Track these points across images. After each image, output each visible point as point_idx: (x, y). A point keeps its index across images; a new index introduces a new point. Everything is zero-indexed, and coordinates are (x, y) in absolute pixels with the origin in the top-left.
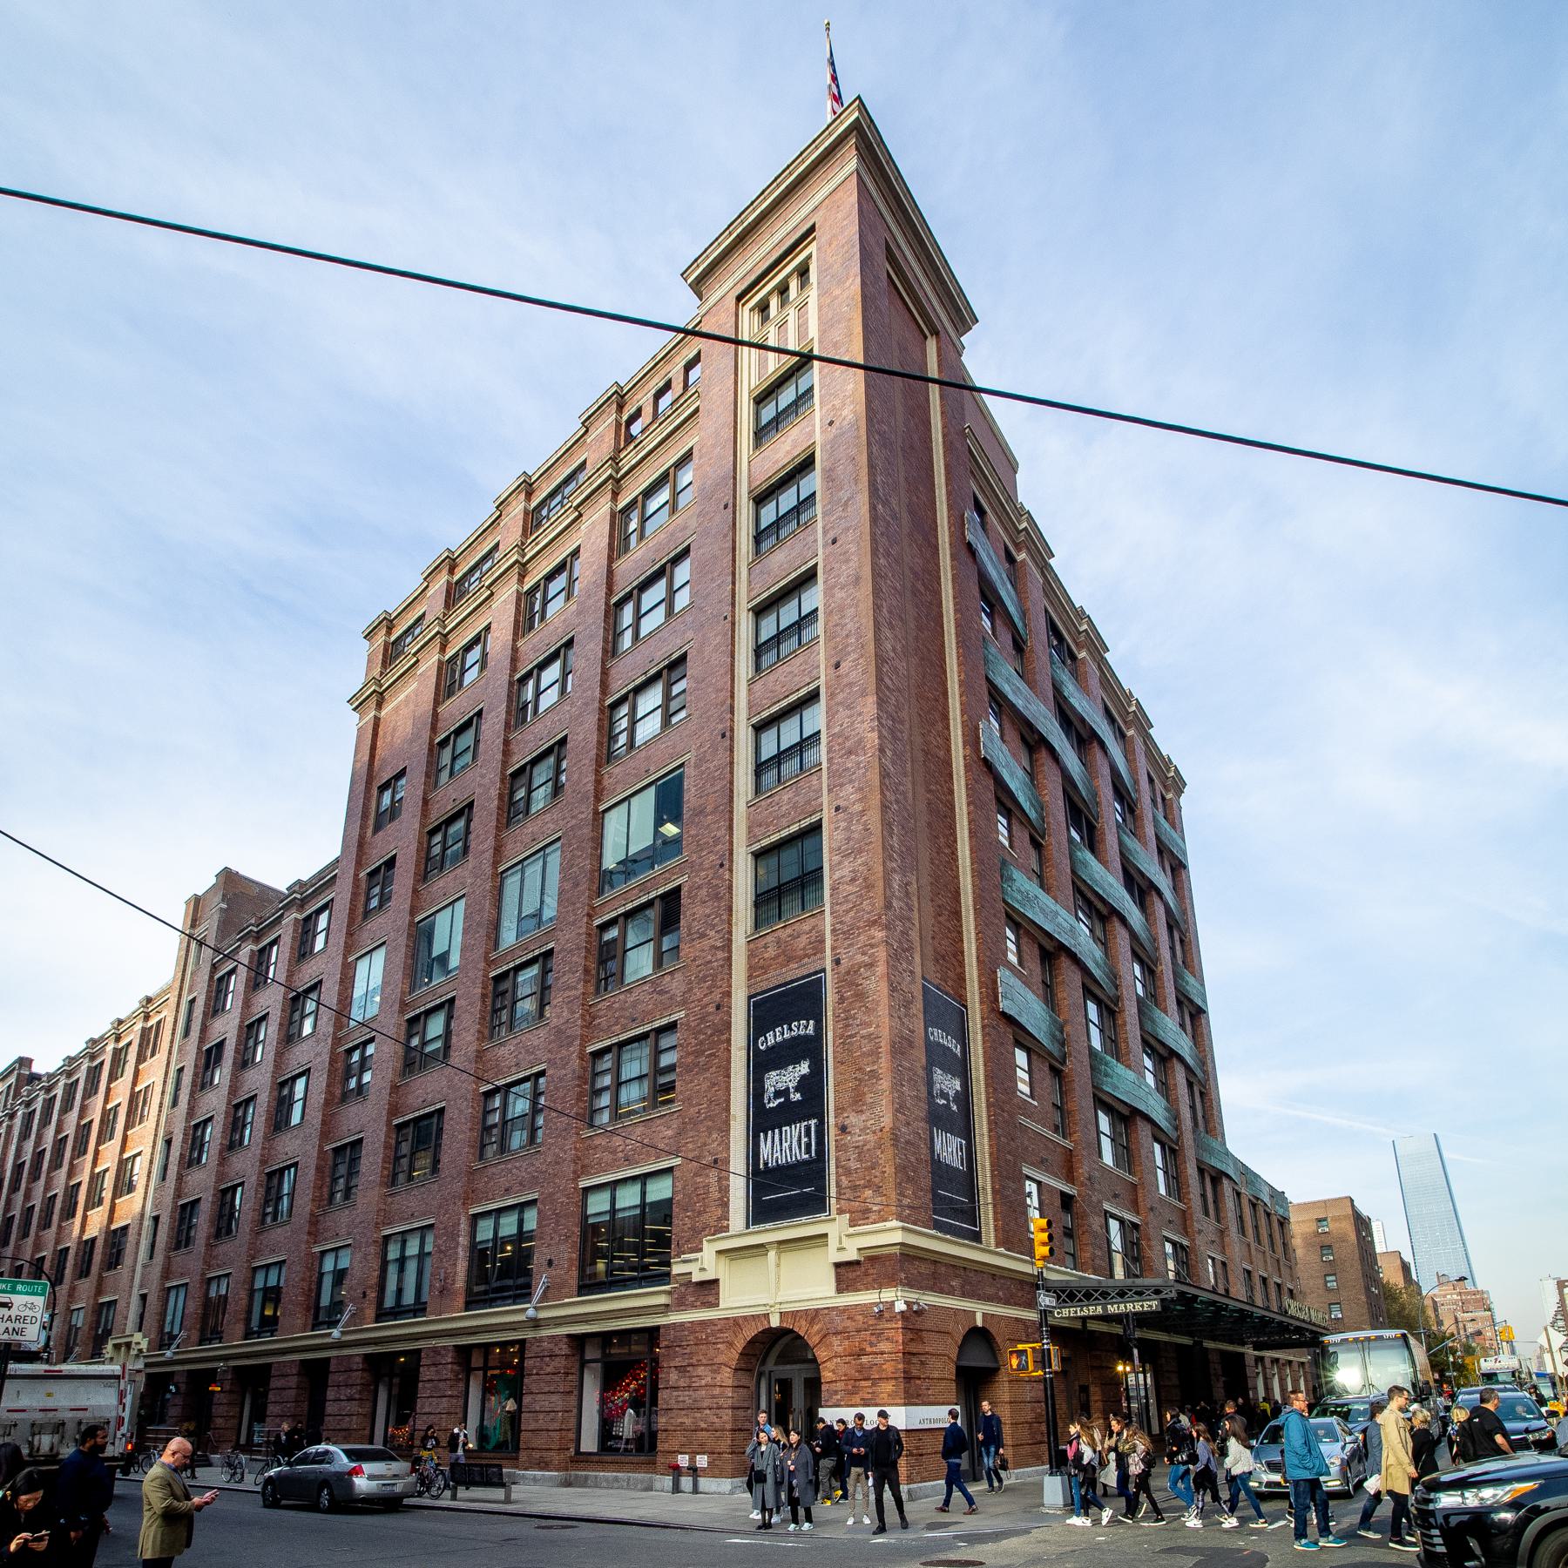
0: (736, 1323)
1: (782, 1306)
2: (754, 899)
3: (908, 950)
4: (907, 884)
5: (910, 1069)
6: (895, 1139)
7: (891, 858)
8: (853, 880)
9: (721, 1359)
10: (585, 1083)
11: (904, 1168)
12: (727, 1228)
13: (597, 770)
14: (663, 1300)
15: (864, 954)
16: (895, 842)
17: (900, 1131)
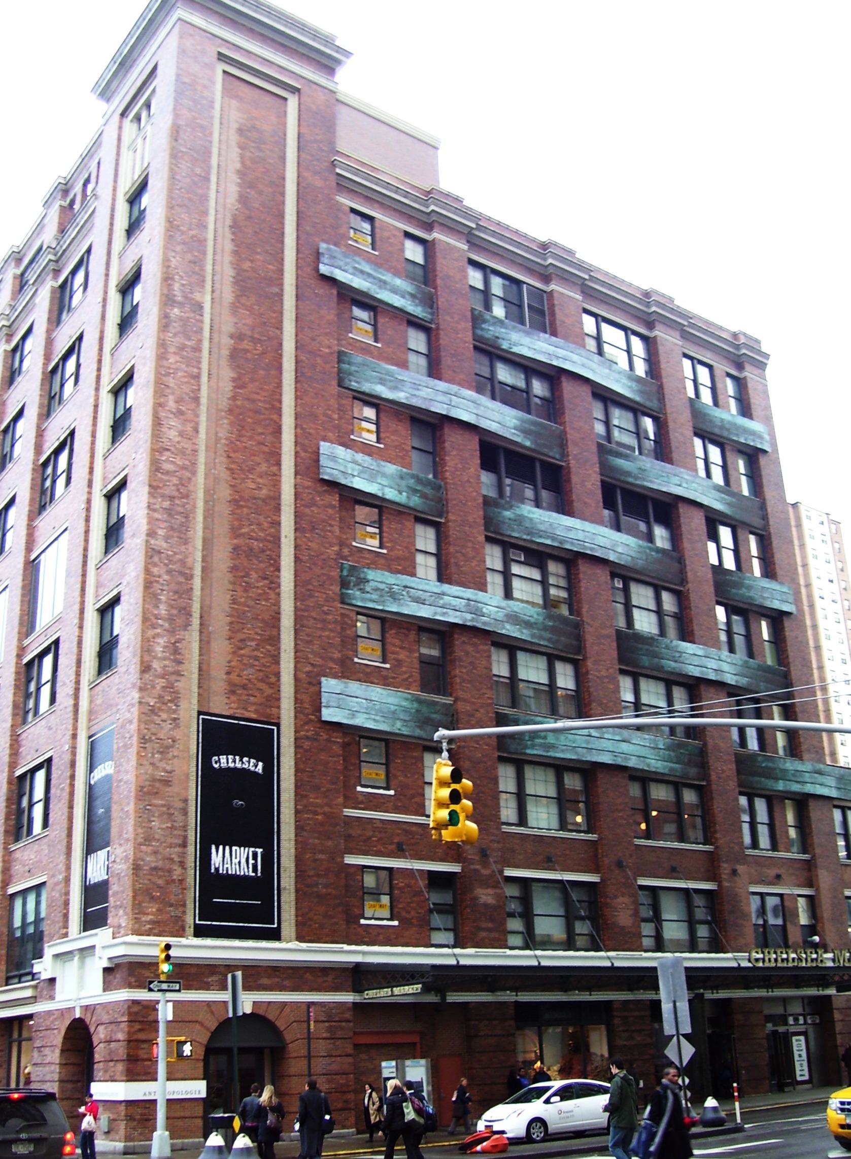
0: (63, 1012)
1: (82, 1001)
2: (98, 649)
3: (170, 701)
4: (175, 642)
5: (163, 806)
6: (136, 868)
7: (154, 627)
8: (128, 647)
9: (54, 1043)
10: (13, 804)
11: (147, 890)
12: (66, 935)
13: (28, 525)
14: (29, 993)
15: (129, 711)
16: (163, 610)
17: (143, 860)
